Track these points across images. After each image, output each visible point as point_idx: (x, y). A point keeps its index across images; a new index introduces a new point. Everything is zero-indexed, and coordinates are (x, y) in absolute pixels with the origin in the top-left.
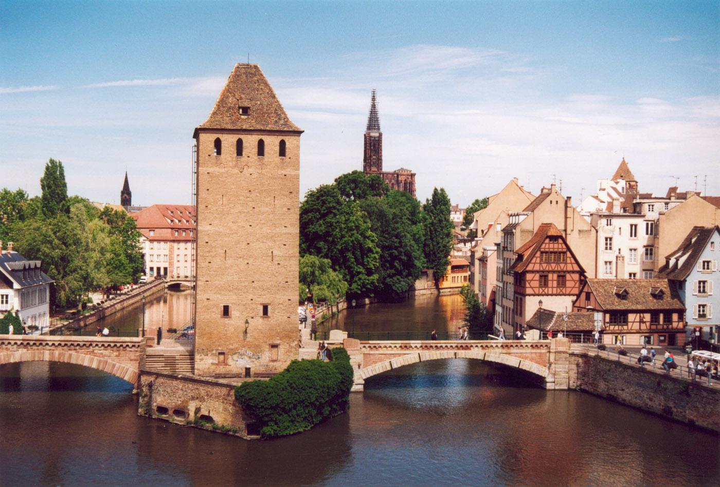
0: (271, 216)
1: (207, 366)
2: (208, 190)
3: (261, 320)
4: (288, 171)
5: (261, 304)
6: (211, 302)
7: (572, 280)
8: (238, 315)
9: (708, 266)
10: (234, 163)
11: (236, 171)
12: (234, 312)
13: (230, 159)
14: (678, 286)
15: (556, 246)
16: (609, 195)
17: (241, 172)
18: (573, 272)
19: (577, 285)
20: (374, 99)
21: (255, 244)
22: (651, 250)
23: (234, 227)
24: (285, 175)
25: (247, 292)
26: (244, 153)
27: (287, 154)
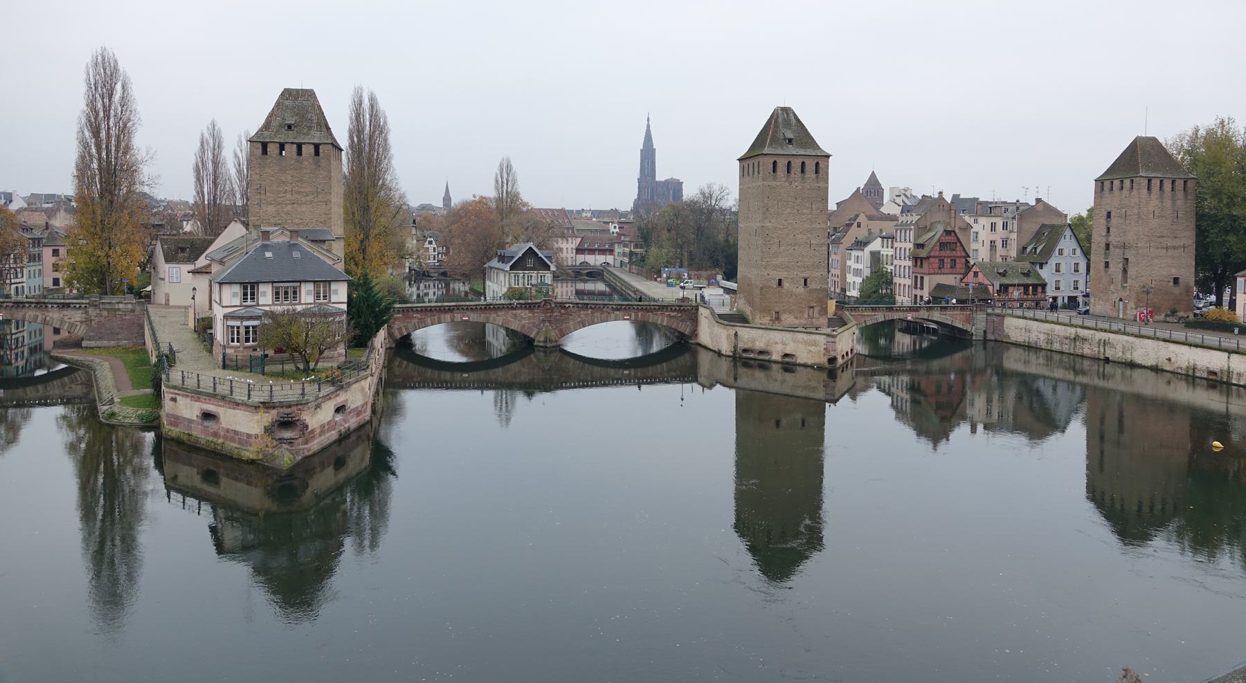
0: (810, 216)
1: (767, 322)
3: (803, 289)
4: (821, 184)
7: (960, 263)
9: (1062, 252)
11: (787, 184)
12: (786, 284)
14: (1038, 267)
15: (950, 238)
16: (903, 201)
18: (961, 257)
19: (964, 266)
20: (648, 120)
22: (1006, 241)
26: (792, 171)
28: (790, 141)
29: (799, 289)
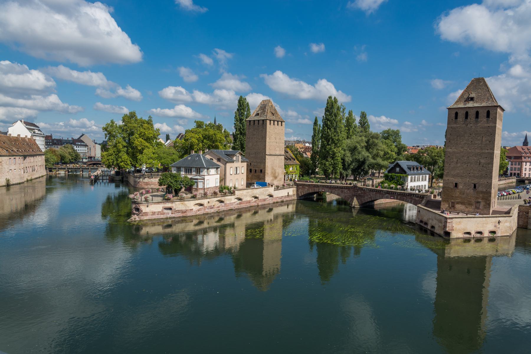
0: (480, 145)
2: (451, 134)
3: (472, 190)
4: (491, 124)
5: (473, 183)
6: (449, 181)
8: (461, 187)
10: (463, 122)
13: (461, 120)
17: (467, 126)
21: (471, 157)
23: (462, 150)
24: (489, 126)
25: (466, 178)
26: (468, 118)
27: (490, 116)
28: (472, 99)
29: (469, 190)
